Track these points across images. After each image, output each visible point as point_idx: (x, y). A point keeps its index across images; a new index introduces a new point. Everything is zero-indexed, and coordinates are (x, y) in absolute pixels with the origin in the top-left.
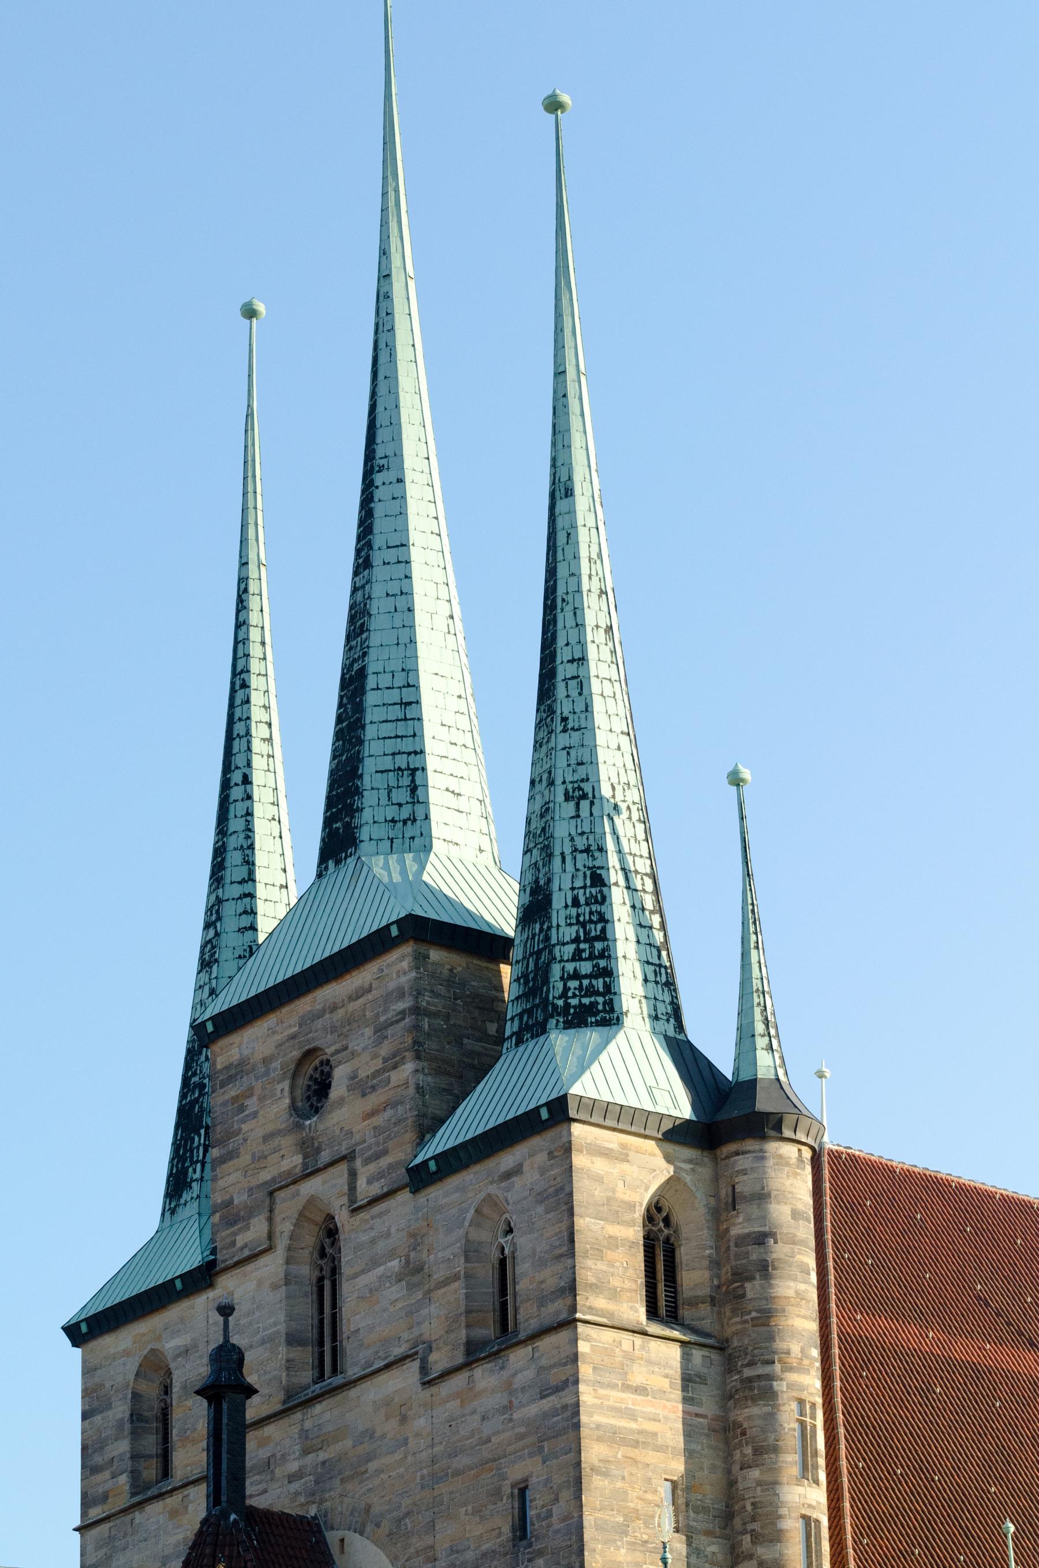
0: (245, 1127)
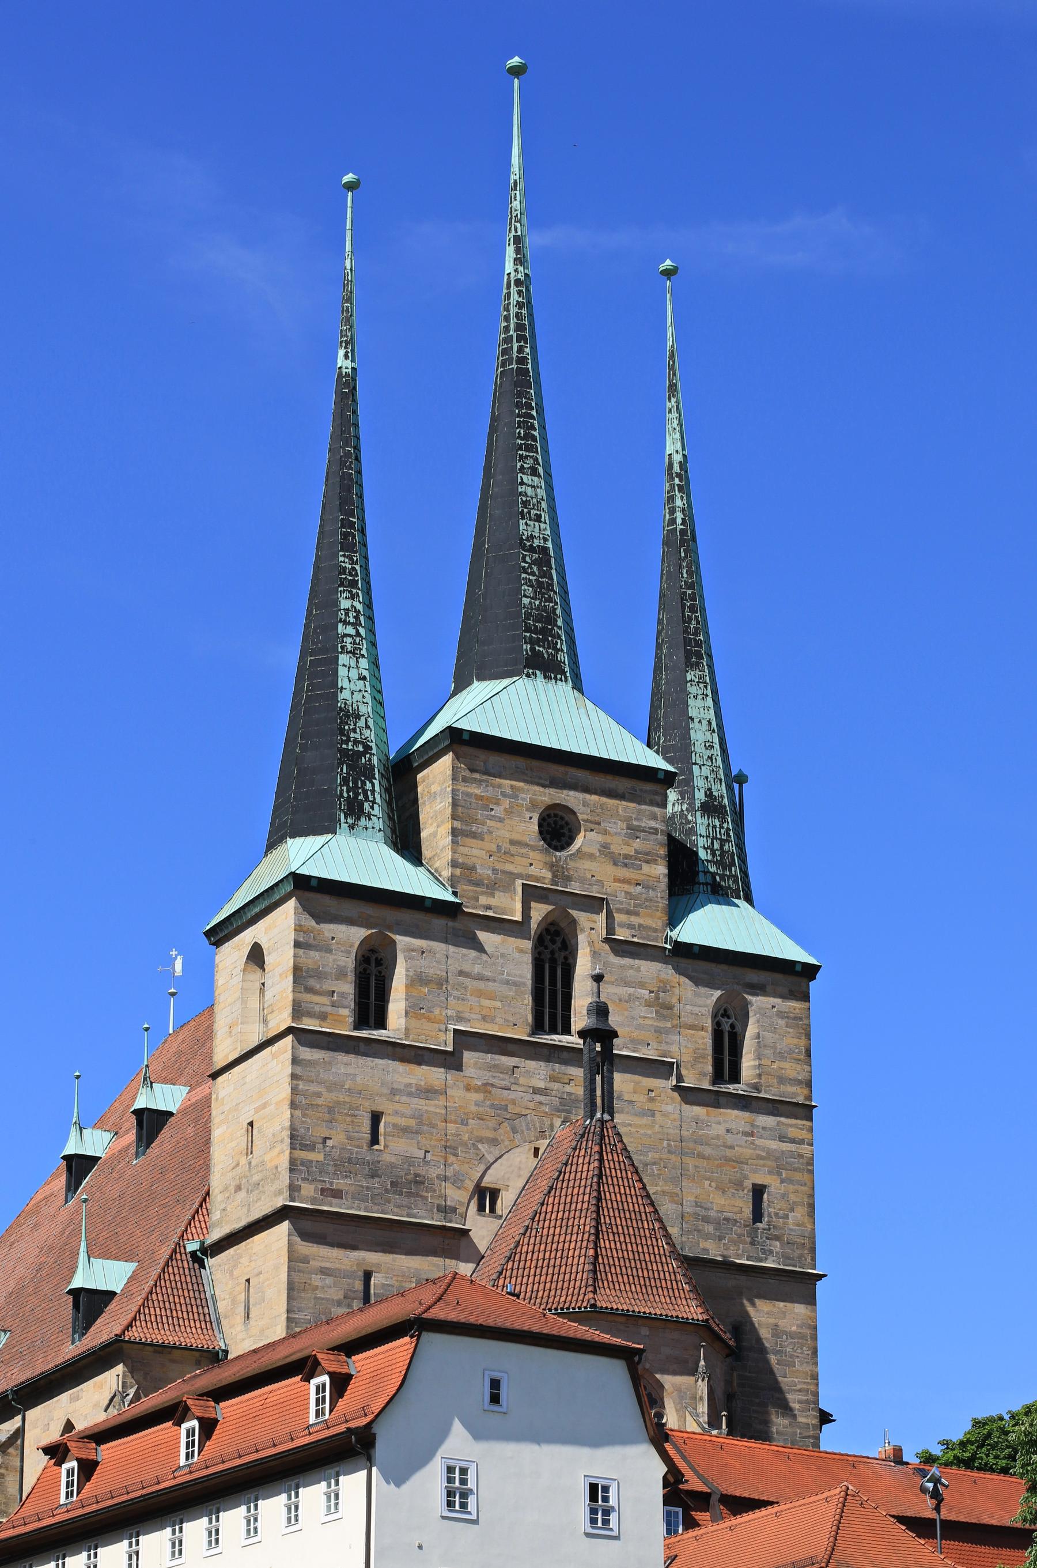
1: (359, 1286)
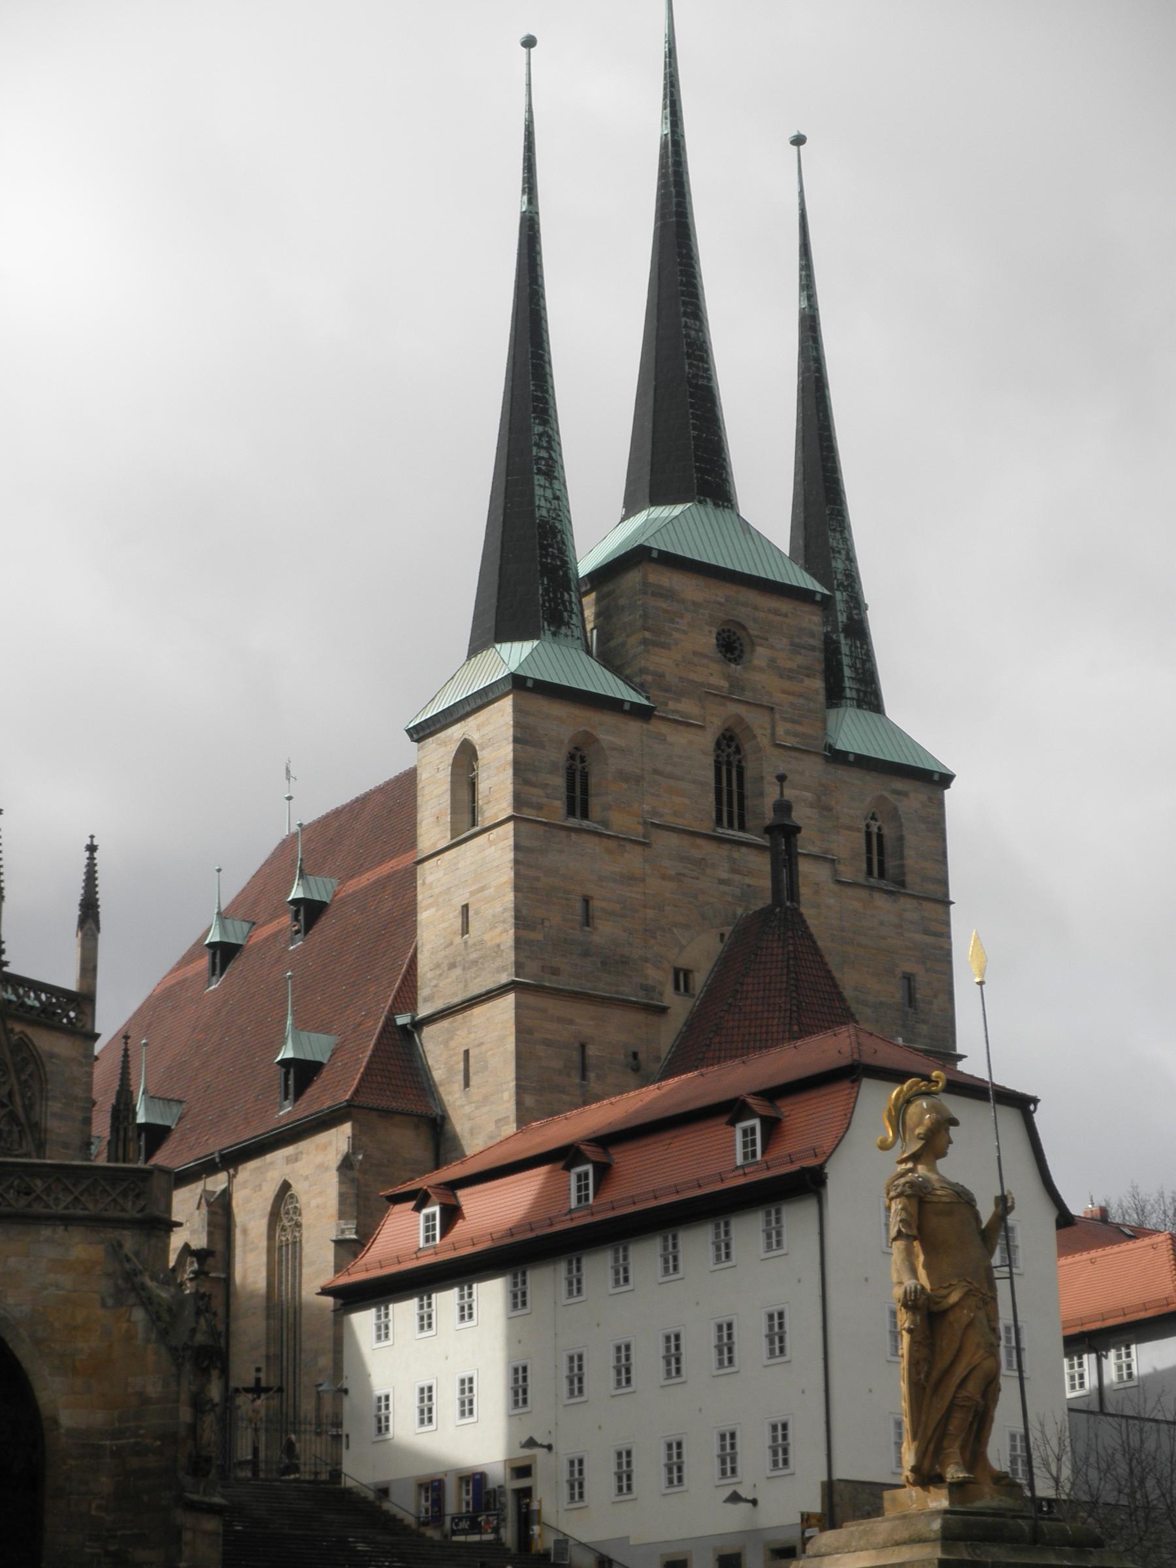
0: (676, 635)
1: (576, 1056)
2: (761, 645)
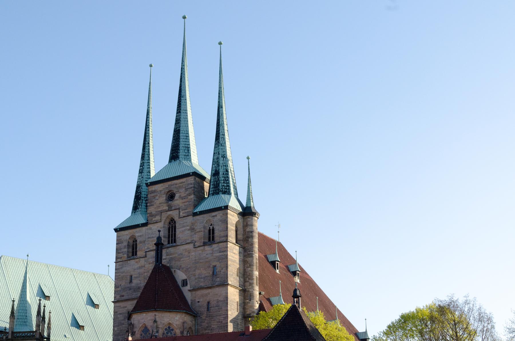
2: (177, 193)
